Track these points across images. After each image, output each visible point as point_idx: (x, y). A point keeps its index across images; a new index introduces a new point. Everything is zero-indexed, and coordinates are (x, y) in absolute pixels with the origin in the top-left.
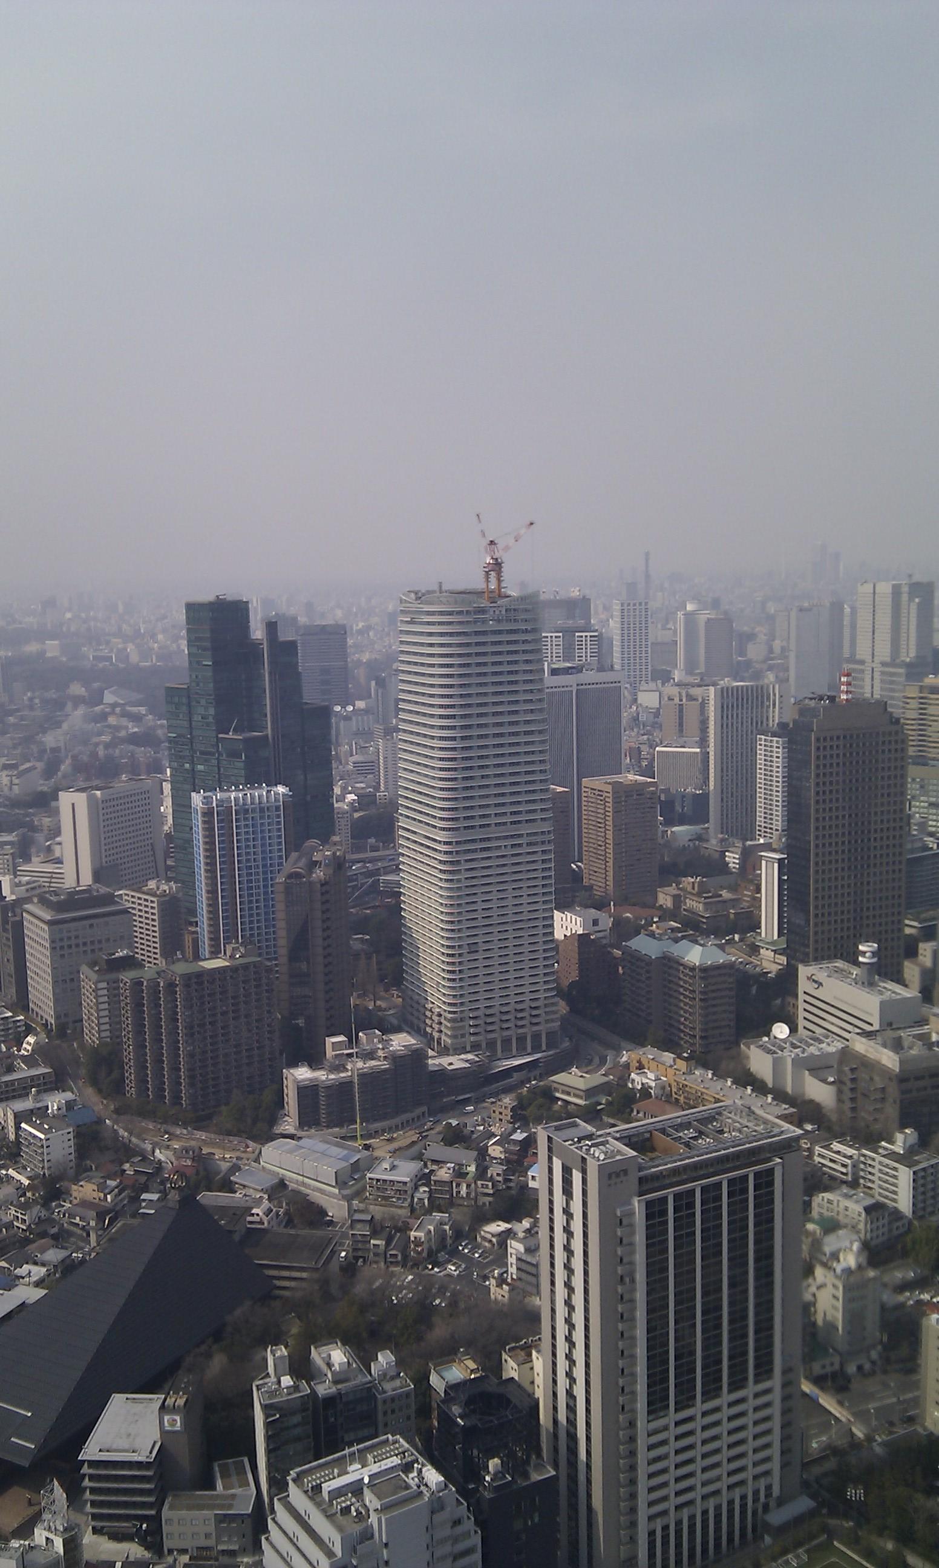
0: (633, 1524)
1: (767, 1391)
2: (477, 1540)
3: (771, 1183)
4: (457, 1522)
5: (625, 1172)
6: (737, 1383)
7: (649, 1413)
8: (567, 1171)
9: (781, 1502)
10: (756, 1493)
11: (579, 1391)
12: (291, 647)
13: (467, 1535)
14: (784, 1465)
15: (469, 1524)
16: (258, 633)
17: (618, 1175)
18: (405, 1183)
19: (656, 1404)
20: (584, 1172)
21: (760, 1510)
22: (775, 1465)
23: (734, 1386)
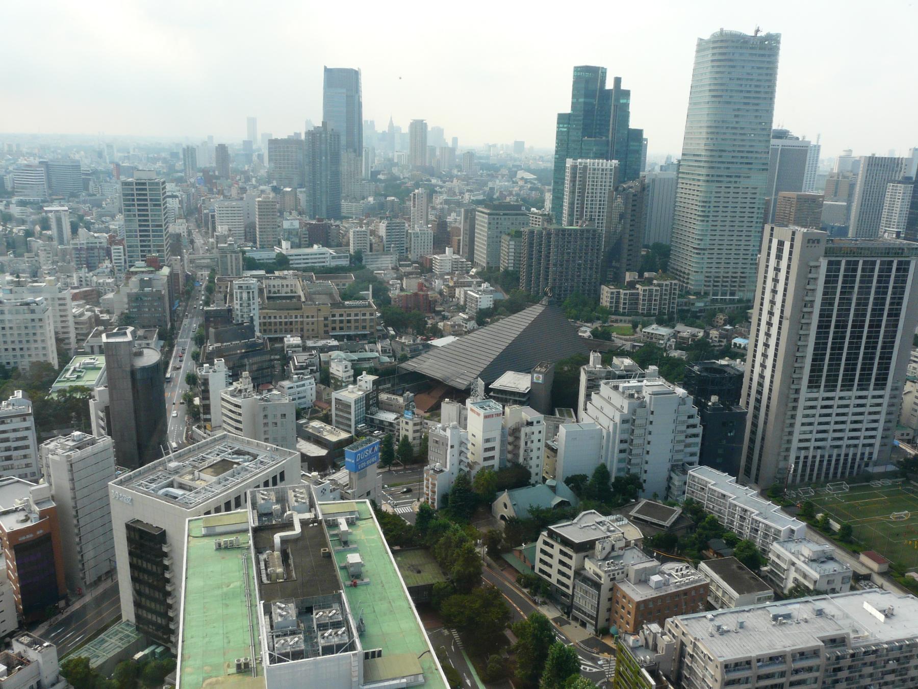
0: (788, 450)
1: (881, 397)
2: (699, 430)
3: (906, 270)
4: (691, 417)
5: (818, 241)
6: (863, 387)
7: (809, 387)
8: (781, 244)
9: (876, 464)
10: (863, 454)
11: (768, 373)
12: (627, 94)
13: (694, 426)
14: (883, 445)
15: (697, 420)
16: (609, 85)
17: (813, 242)
18: (663, 336)
19: (814, 383)
20: (793, 240)
21: (863, 466)
22: (877, 442)
23: (862, 387)
